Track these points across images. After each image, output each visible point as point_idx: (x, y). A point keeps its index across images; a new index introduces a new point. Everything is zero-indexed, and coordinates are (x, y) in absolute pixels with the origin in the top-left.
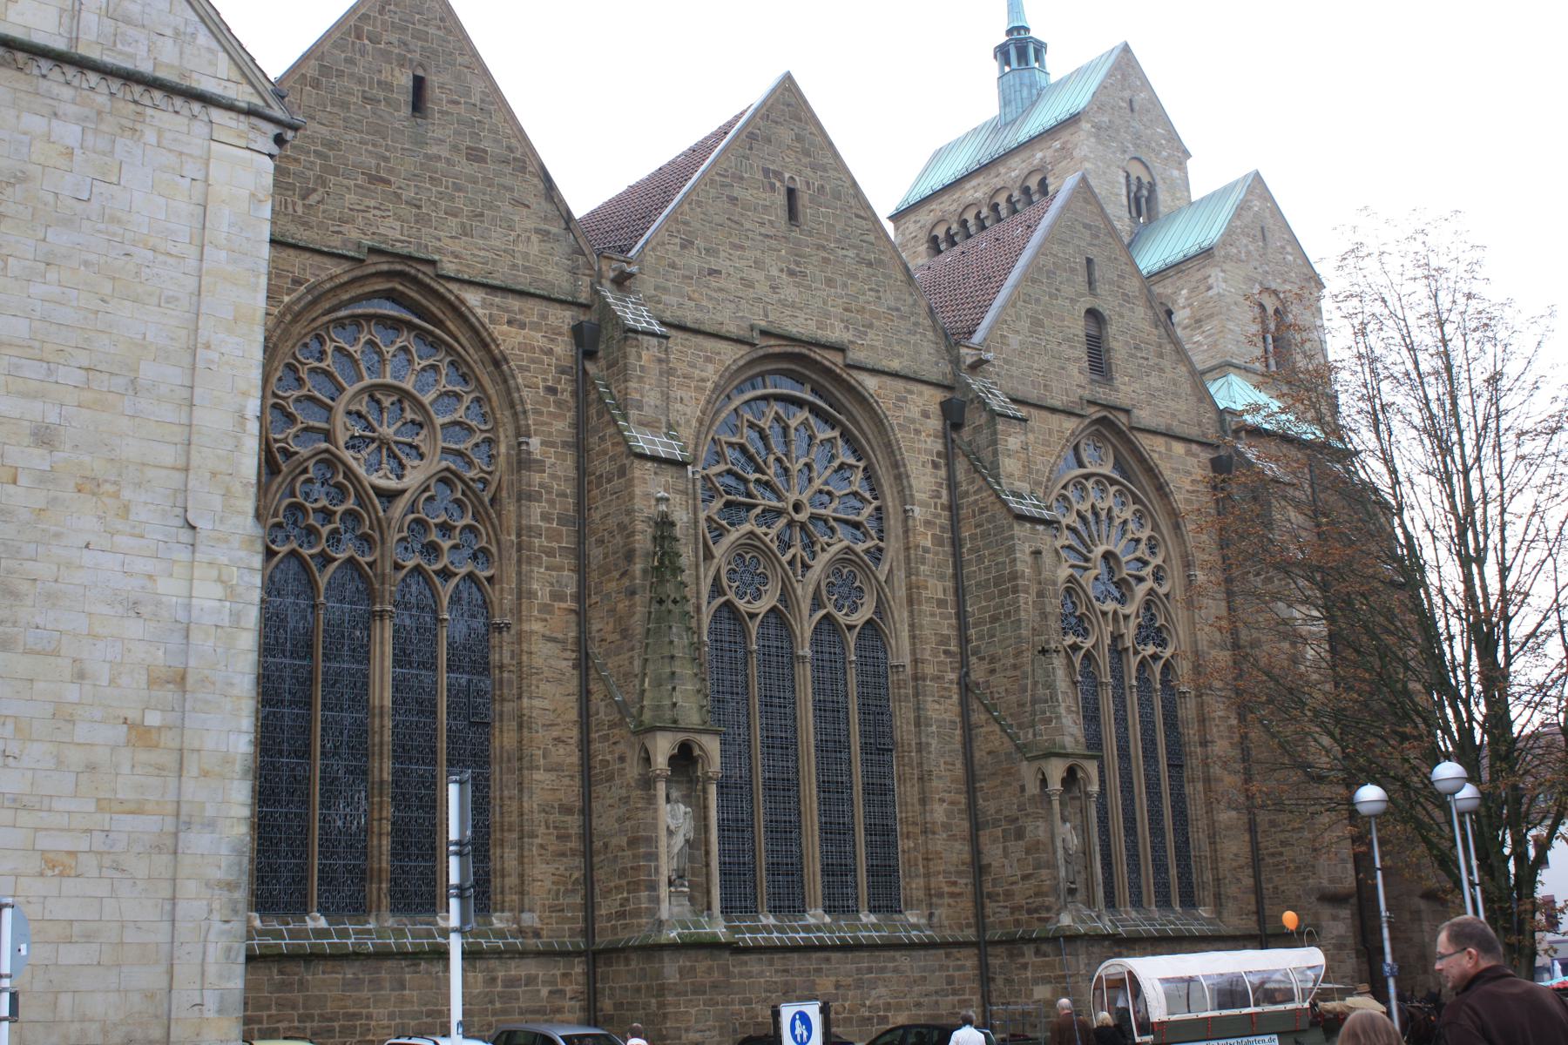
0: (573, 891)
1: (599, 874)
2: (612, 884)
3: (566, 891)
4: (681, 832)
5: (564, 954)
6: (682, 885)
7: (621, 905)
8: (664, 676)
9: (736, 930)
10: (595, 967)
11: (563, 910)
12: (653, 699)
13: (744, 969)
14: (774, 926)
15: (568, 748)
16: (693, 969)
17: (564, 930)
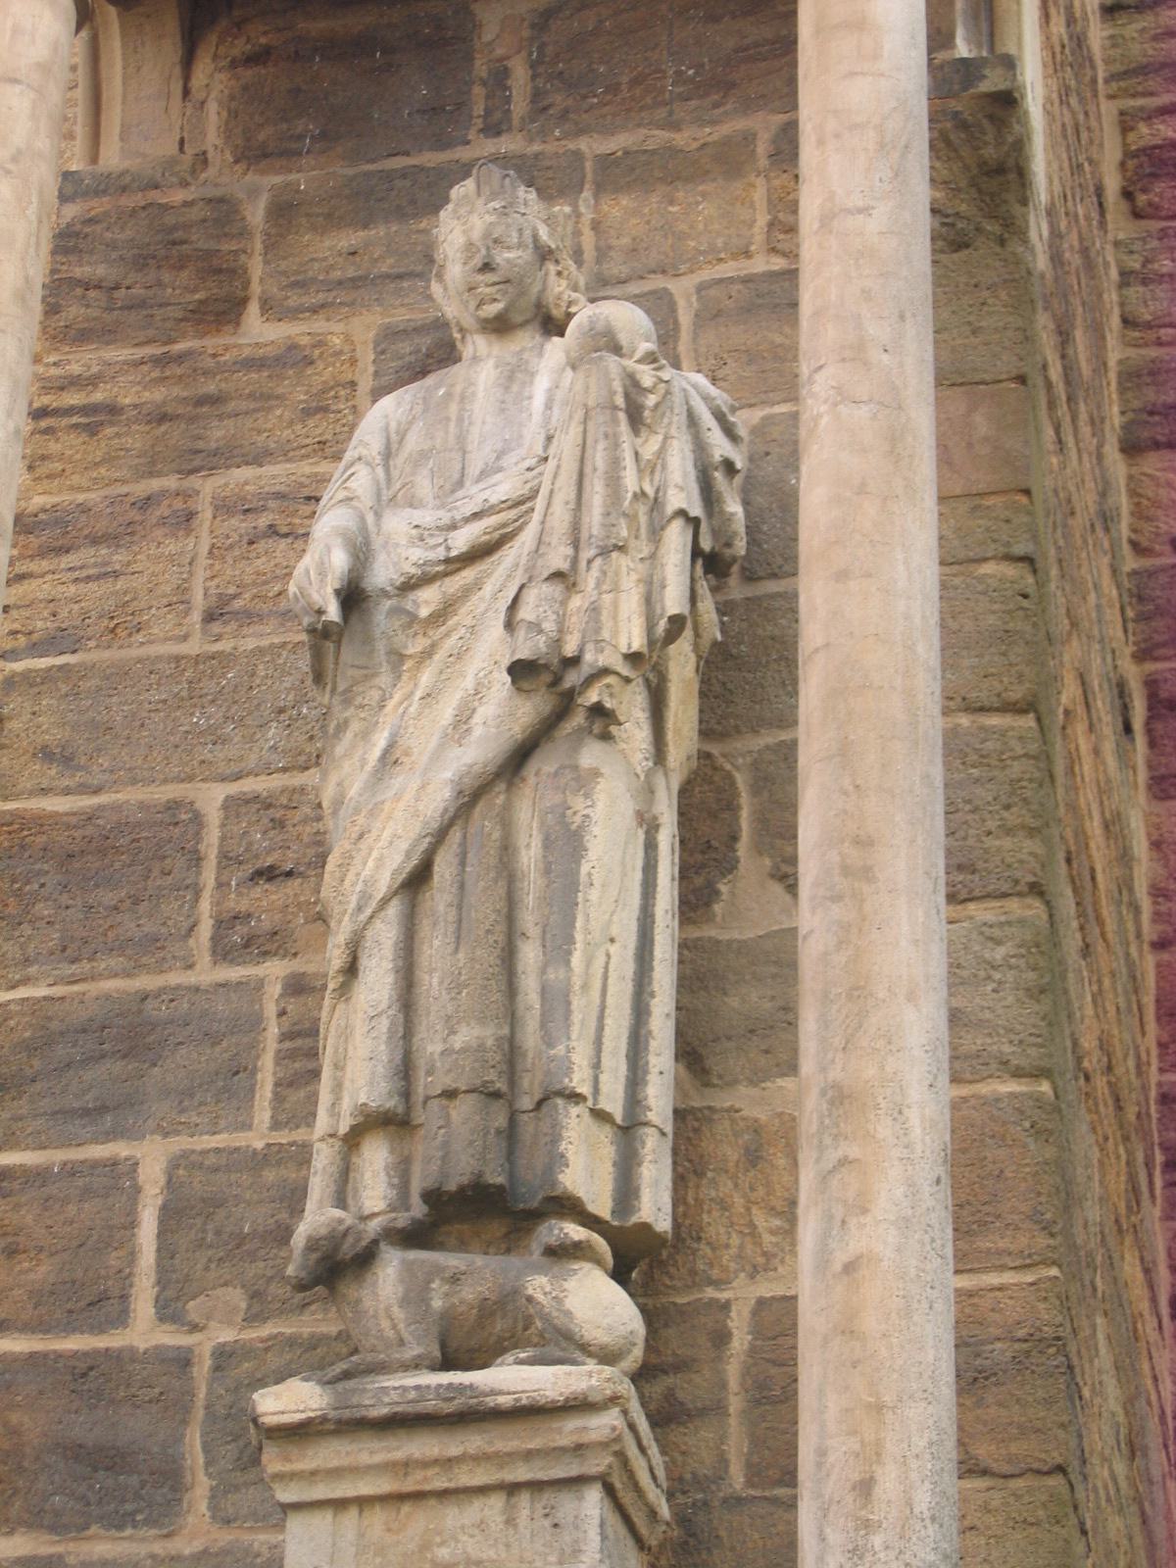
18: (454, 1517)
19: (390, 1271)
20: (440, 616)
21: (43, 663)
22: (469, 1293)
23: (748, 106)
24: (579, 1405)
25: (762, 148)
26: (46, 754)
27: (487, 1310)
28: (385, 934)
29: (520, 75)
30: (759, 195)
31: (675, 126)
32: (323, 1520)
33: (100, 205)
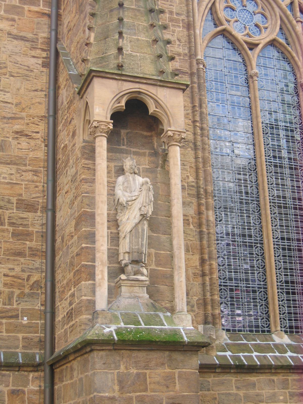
0: (31, 295)
1: (59, 276)
2: (65, 282)
3: (22, 295)
4: (137, 205)
5: (18, 367)
6: (137, 273)
7: (71, 304)
8: (111, 27)
9: (245, 348)
10: (52, 384)
11: (17, 317)
12: (97, 53)
13: (252, 392)
14: (288, 345)
15: (32, 142)
16: (141, 378)
17: (17, 339)
18: (135, 288)
19: (130, 267)
20: (131, 205)
21: (86, 195)
22: (136, 269)
23: (146, 149)
24: (146, 281)
25: (147, 154)
26: (87, 205)
27: (137, 271)
28: (128, 236)
29: (125, 140)
30: (147, 159)
31: (139, 149)
32: (124, 287)
33: (87, 144)
